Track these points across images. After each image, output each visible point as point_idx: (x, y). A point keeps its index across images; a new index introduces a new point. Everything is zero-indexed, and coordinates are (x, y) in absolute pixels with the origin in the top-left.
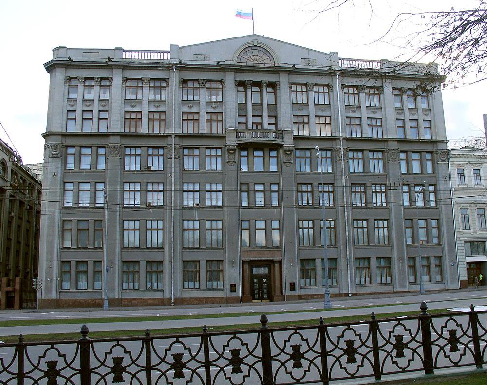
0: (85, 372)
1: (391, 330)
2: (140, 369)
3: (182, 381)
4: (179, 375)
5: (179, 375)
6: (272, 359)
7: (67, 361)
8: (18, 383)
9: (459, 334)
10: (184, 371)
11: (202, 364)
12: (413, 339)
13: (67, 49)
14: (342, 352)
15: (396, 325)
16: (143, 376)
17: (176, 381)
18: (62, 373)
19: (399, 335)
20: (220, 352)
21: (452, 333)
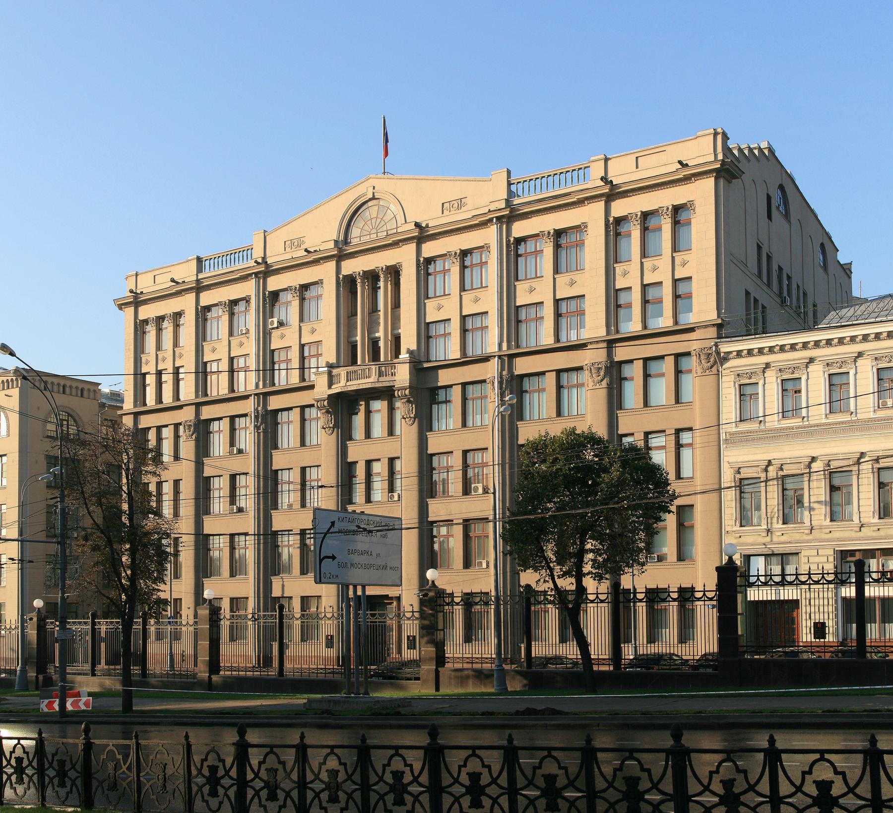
0: (436, 790)
1: (386, 762)
2: (449, 790)
3: (403, 809)
4: (399, 802)
5: (399, 802)
6: (442, 790)
7: (849, 781)
8: (772, 810)
9: (485, 779)
10: (483, 798)
11: (357, 787)
12: (494, 781)
13: (315, 518)
14: (488, 790)
15: (469, 756)
16: (504, 801)
17: (395, 808)
18: (488, 790)
19: (474, 772)
20: (798, 783)
21: (475, 777)
